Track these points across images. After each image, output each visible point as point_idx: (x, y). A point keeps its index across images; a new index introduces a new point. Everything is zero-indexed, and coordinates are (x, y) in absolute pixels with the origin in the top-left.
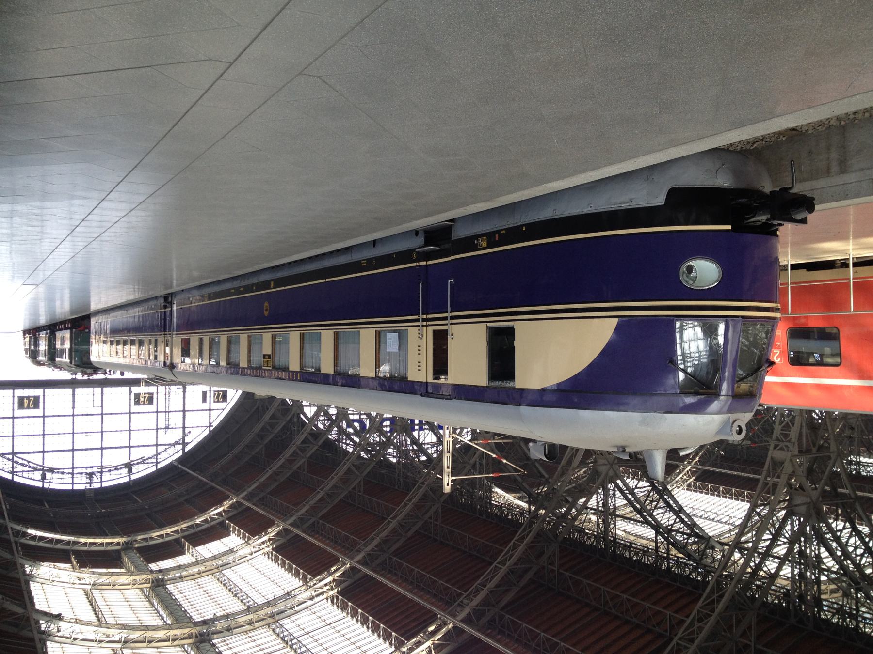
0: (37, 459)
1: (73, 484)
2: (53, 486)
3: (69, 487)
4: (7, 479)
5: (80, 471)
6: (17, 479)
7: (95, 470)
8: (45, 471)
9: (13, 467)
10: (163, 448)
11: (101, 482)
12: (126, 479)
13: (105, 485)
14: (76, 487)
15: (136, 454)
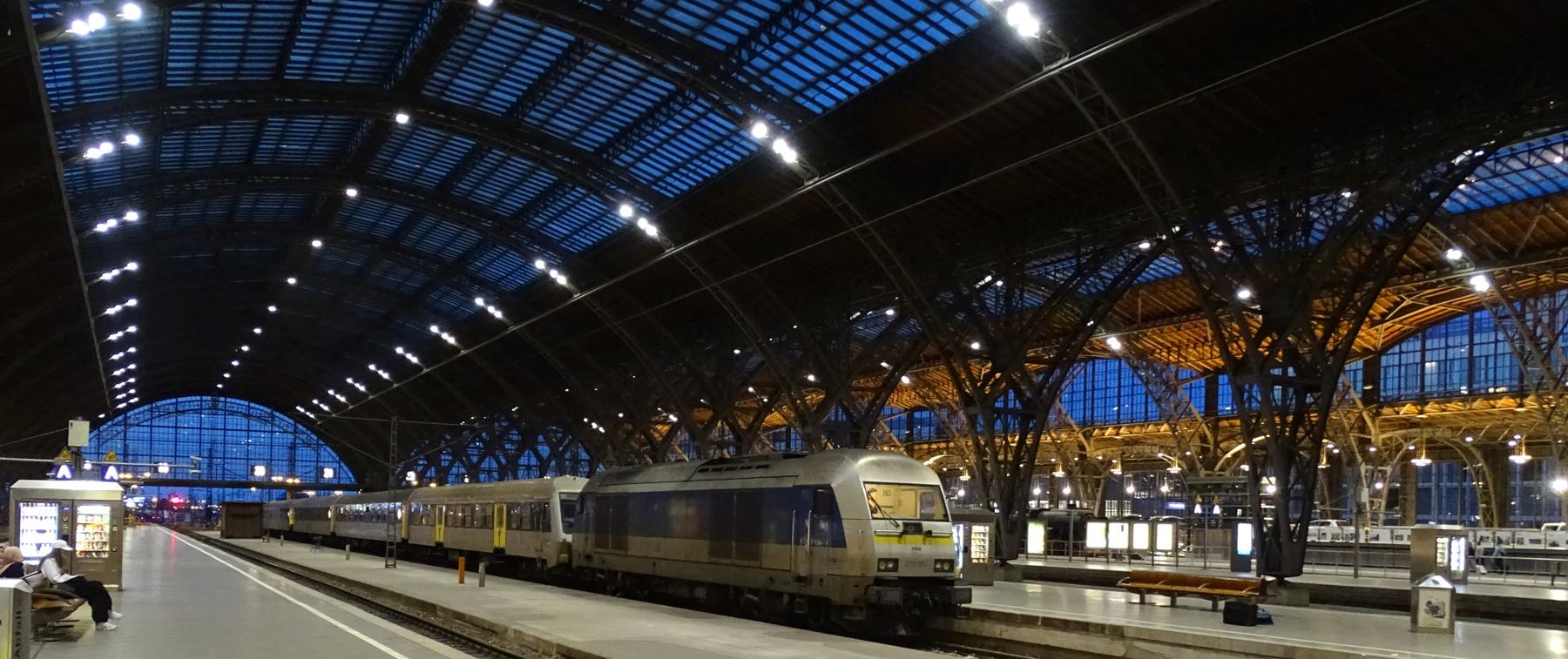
0: (255, 425)
1: (225, 402)
2: (242, 402)
3: (228, 400)
4: (276, 411)
5: (220, 412)
6: (269, 411)
7: (206, 412)
8: (248, 416)
9: (272, 420)
10: (145, 423)
11: (201, 401)
12: (180, 399)
13: (198, 398)
14: (222, 399)
15: (171, 421)
